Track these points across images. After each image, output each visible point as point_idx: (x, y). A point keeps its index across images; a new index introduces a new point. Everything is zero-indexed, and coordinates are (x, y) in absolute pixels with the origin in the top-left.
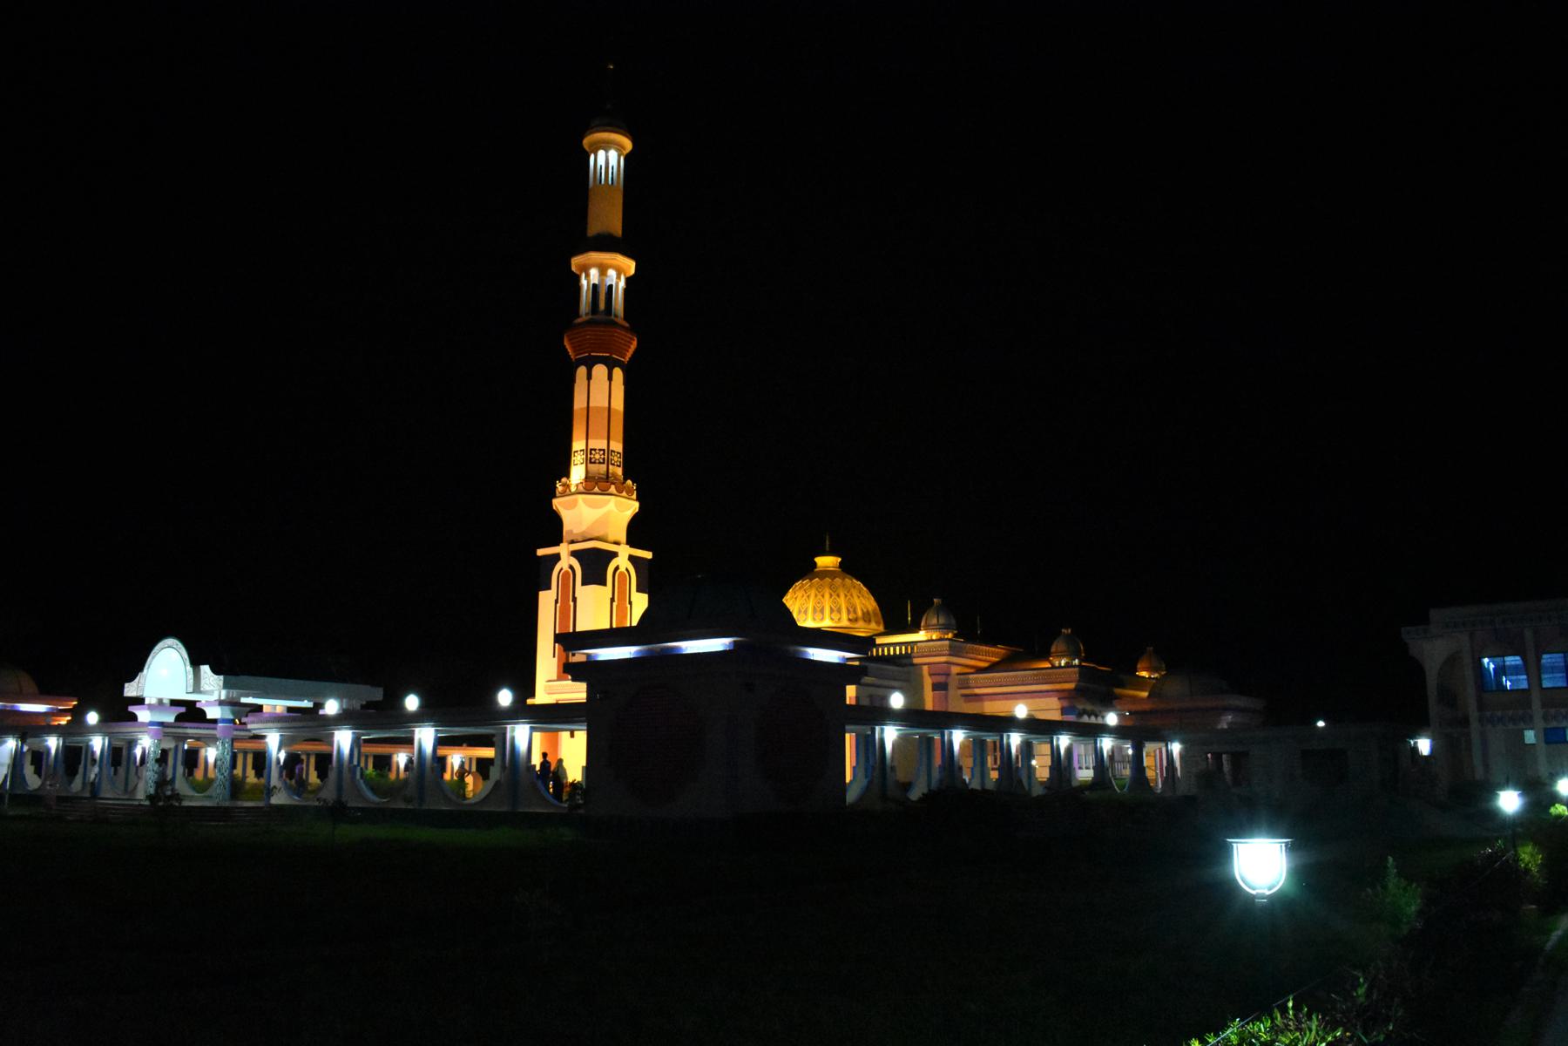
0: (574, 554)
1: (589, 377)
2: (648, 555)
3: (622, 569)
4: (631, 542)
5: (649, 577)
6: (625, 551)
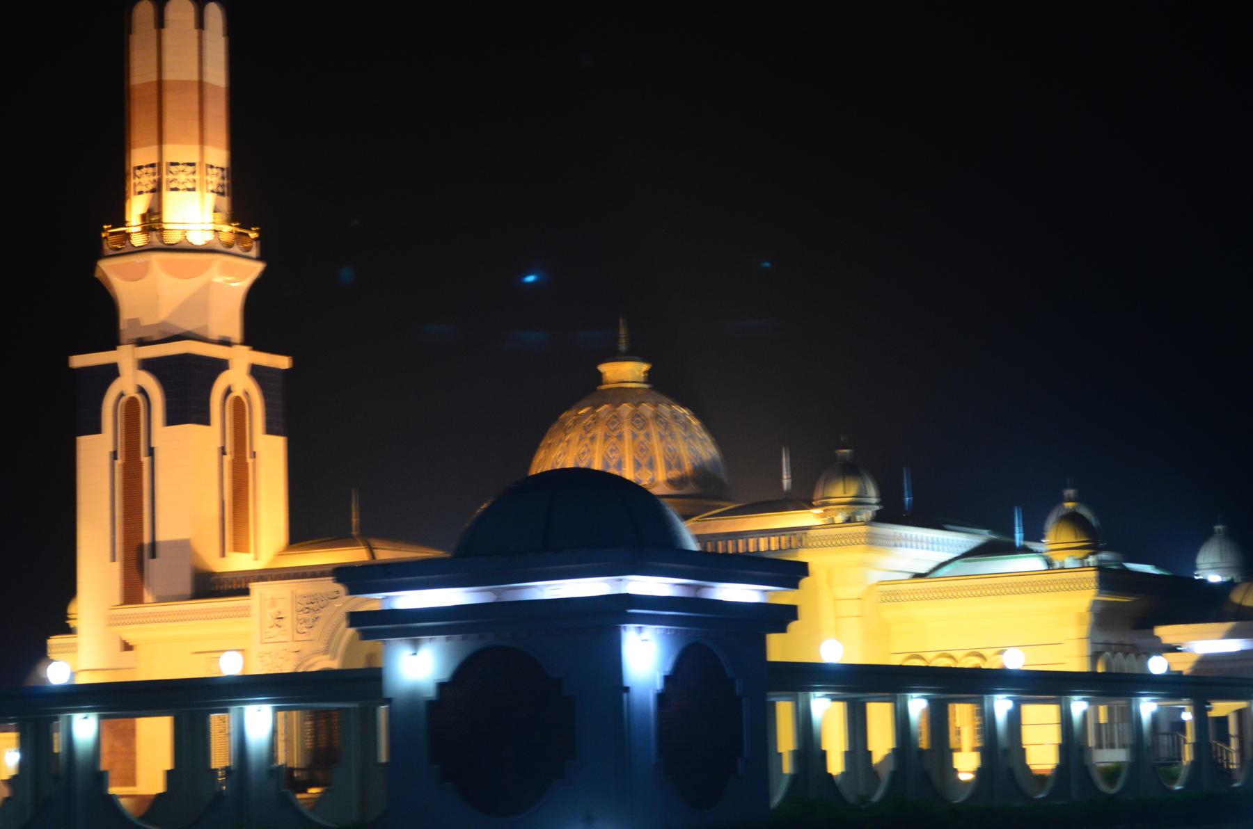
0: (148, 365)
1: (160, 23)
2: (282, 362)
3: (238, 392)
4: (254, 336)
5: (289, 407)
6: (242, 359)
